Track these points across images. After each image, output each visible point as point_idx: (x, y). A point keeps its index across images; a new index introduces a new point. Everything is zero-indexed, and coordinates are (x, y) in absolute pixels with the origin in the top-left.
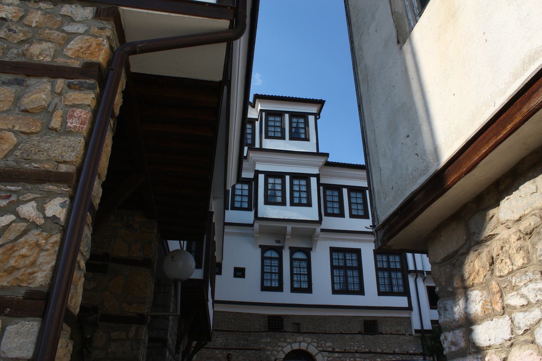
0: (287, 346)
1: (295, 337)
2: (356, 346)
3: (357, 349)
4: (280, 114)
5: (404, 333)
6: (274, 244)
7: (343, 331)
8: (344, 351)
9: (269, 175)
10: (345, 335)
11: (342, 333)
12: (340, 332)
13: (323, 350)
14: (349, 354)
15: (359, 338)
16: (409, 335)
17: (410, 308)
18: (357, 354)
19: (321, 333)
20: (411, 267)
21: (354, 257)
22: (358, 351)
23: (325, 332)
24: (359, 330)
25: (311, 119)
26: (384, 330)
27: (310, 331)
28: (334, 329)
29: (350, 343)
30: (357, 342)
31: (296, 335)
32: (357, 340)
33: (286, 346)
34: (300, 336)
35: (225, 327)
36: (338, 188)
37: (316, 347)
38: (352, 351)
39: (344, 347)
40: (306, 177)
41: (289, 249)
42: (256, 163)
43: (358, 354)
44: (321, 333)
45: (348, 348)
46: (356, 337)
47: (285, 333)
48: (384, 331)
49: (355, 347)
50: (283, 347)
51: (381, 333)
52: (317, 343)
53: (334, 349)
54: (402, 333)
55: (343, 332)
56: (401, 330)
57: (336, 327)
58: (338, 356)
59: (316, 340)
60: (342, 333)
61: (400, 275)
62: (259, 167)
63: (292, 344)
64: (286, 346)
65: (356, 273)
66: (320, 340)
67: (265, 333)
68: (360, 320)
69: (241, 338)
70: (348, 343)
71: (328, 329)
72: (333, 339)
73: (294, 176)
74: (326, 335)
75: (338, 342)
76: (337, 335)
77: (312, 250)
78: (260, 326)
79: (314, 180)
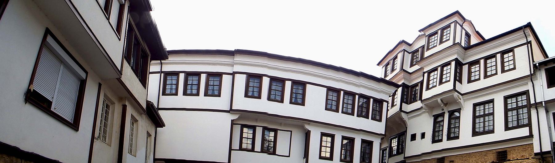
5: (528, 157)
16: (532, 158)
17: (531, 136)
20: (532, 102)
41: (448, 112)
51: (509, 160)
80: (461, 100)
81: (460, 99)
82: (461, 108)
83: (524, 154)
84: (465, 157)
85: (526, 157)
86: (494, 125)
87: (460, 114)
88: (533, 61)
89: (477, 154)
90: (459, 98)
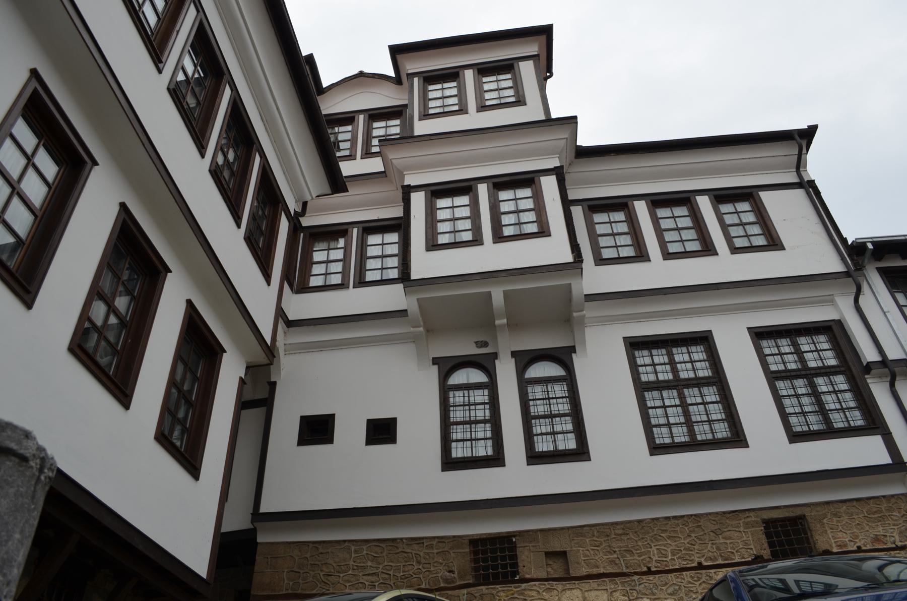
1: (555, 591)
4: (452, 75)
5: (899, 544)
6: (467, 348)
7: (703, 560)
9: (437, 191)
10: (713, 571)
11: (700, 567)
12: (695, 564)
21: (698, 353)
23: (649, 568)
24: (755, 553)
25: (527, 70)
26: (833, 541)
27: (602, 571)
28: (675, 558)
34: (571, 589)
35: (348, 585)
36: (622, 204)
40: (528, 180)
42: (404, 173)
47: (524, 586)
48: (834, 545)
54: (894, 543)
55: (705, 564)
56: (888, 534)
57: (680, 550)
59: (624, 595)
60: (700, 567)
61: (841, 382)
62: (411, 180)
65: (711, 394)
66: (635, 594)
67: (465, 591)
68: (749, 520)
71: (655, 558)
72: (677, 587)
73: (501, 183)
75: (694, 596)
76: (688, 573)
77: (575, 352)
78: (450, 572)
79: (549, 185)
82: (574, 347)
83: (880, 530)
84: (624, 538)
85: (894, 543)
87: (569, 368)
88: (844, 241)
89: (678, 525)
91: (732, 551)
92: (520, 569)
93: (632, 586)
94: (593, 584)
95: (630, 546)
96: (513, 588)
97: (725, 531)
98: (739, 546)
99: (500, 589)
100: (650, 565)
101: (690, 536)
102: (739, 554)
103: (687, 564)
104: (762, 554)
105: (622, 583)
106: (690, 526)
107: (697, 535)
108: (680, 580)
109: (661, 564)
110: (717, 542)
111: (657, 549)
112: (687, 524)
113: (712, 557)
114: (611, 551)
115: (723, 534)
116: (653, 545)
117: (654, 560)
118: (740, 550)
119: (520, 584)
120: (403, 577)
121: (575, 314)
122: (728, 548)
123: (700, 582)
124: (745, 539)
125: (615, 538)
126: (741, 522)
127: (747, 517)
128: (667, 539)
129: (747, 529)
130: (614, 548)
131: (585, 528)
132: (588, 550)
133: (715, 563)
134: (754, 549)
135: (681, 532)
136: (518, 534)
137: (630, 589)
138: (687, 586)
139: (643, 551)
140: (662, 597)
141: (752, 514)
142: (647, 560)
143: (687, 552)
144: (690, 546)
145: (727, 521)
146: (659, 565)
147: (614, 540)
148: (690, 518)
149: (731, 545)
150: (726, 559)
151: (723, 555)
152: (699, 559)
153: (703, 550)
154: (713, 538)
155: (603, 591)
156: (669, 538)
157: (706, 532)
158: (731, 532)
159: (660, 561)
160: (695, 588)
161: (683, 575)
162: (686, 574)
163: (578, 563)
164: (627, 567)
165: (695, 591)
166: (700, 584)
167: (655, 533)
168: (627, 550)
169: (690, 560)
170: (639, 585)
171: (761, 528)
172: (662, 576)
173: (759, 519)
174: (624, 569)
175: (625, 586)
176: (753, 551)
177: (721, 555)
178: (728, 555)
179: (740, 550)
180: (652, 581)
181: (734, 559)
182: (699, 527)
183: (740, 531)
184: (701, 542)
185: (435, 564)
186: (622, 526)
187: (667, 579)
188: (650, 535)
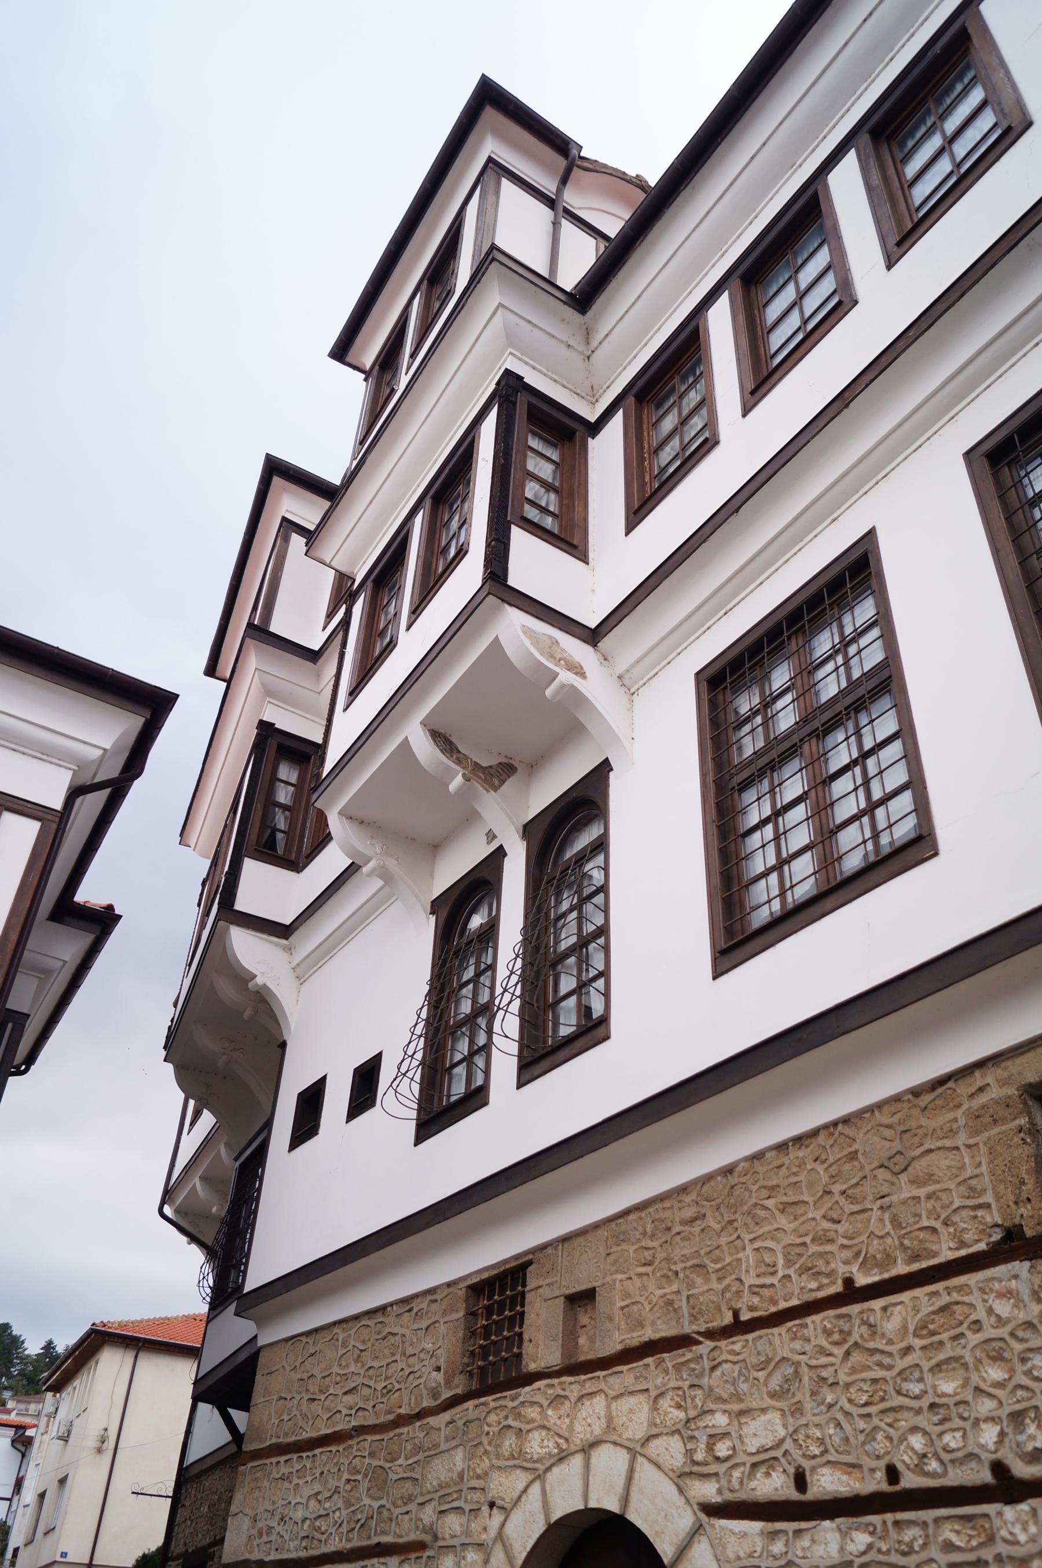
0: (524, 1498)
2: (985, 1406)
3: (1002, 1434)
8: (885, 1487)
10: (877, 1304)
12: (838, 1288)
13: (729, 1496)
14: (928, 1515)
15: (1003, 1308)
18: (1009, 1512)
19: (710, 1334)
22: (1022, 1470)
24: (1000, 1222)
27: (649, 1334)
28: (791, 1272)
29: (928, 1377)
30: (997, 1358)
31: (574, 1392)
32: (990, 1333)
33: (519, 1498)
34: (591, 1394)
37: (681, 1478)
38: (957, 1477)
39: (880, 1444)
43: (1024, 1507)
44: (710, 1334)
45: (917, 1442)
46: (975, 1298)
49: (977, 1422)
50: (506, 1511)
52: (685, 1431)
53: (800, 1481)
55: (862, 1280)
58: (842, 1549)
59: (679, 1407)
63: (549, 1469)
64: (519, 1498)
68: (982, 1099)
69: (366, 1475)
70: (916, 1388)
71: (750, 1280)
74: (737, 1343)
76: (817, 1318)
77: (612, 769)
80: (580, 673)
81: (580, 673)
84: (696, 1229)
86: (916, 784)
90: (551, 656)
91: (933, 1223)
92: (528, 1349)
93: (697, 1377)
94: (626, 1376)
95: (702, 1252)
96: (507, 1400)
97: (914, 1159)
98: (952, 1203)
99: (493, 1405)
100: (740, 1306)
101: (829, 1193)
102: (951, 1230)
103: (818, 1289)
104: (1017, 1221)
105: (678, 1367)
106: (831, 1160)
107: (844, 1187)
108: (797, 1345)
109: (762, 1297)
110: (894, 1198)
111: (757, 1250)
112: (823, 1157)
113: (878, 1256)
114: (670, 1273)
115: (910, 1169)
116: (747, 1237)
117: (747, 1285)
118: (956, 1218)
119: (518, 1390)
120: (385, 1391)
121: (548, 692)
122: (920, 1216)
123: (846, 1346)
124: (969, 1172)
125: (679, 1233)
126: (959, 1113)
127: (981, 1089)
128: (777, 1212)
129: (977, 1133)
130: (675, 1263)
131: (631, 1217)
132: (631, 1278)
133: (886, 1276)
134: (993, 1206)
135: (811, 1185)
136: (531, 1257)
137: (692, 1386)
138: (814, 1362)
139: (728, 1260)
140: (754, 1405)
141: (989, 1077)
142: (734, 1289)
143: (821, 1249)
144: (826, 1225)
145: (924, 1122)
146: (756, 1300)
147: (678, 1238)
148: (832, 1134)
149: (929, 1206)
150: (915, 1257)
151: (906, 1242)
152: (847, 1268)
153: (858, 1234)
154: (885, 1190)
155: (642, 1398)
156: (784, 1208)
157: (867, 1168)
158: (932, 1155)
159: (762, 1286)
160: (831, 1369)
161: (806, 1326)
162: (813, 1322)
163: (611, 1319)
164: (694, 1318)
165: (831, 1381)
166: (847, 1354)
167: (754, 1201)
168: (698, 1266)
169: (828, 1275)
170: (713, 1369)
171: (1017, 1122)
172: (761, 1337)
173: (1011, 1091)
174: (686, 1323)
175: (682, 1378)
176: (991, 1214)
177: (902, 1244)
178: (920, 1241)
179: (956, 1218)
180: (738, 1354)
181: (935, 1254)
182: (853, 1156)
183: (957, 1148)
184: (856, 1208)
185: (422, 1355)
186: (693, 1196)
187: (771, 1344)
188: (745, 1208)
